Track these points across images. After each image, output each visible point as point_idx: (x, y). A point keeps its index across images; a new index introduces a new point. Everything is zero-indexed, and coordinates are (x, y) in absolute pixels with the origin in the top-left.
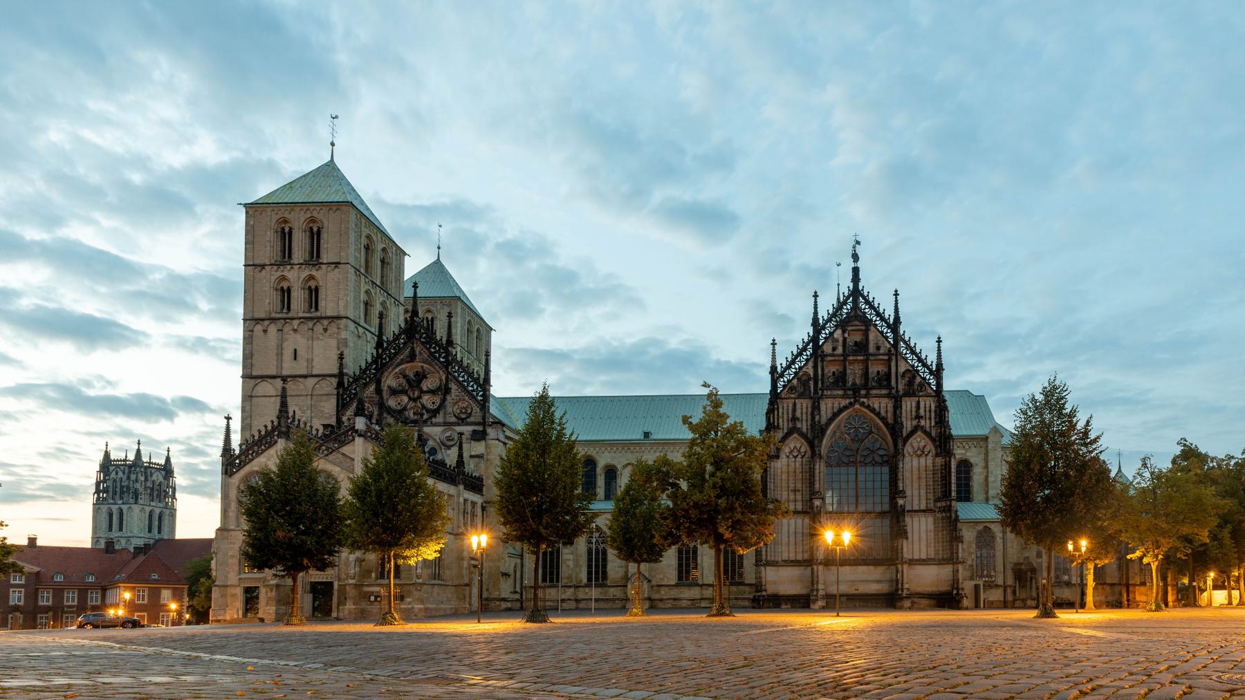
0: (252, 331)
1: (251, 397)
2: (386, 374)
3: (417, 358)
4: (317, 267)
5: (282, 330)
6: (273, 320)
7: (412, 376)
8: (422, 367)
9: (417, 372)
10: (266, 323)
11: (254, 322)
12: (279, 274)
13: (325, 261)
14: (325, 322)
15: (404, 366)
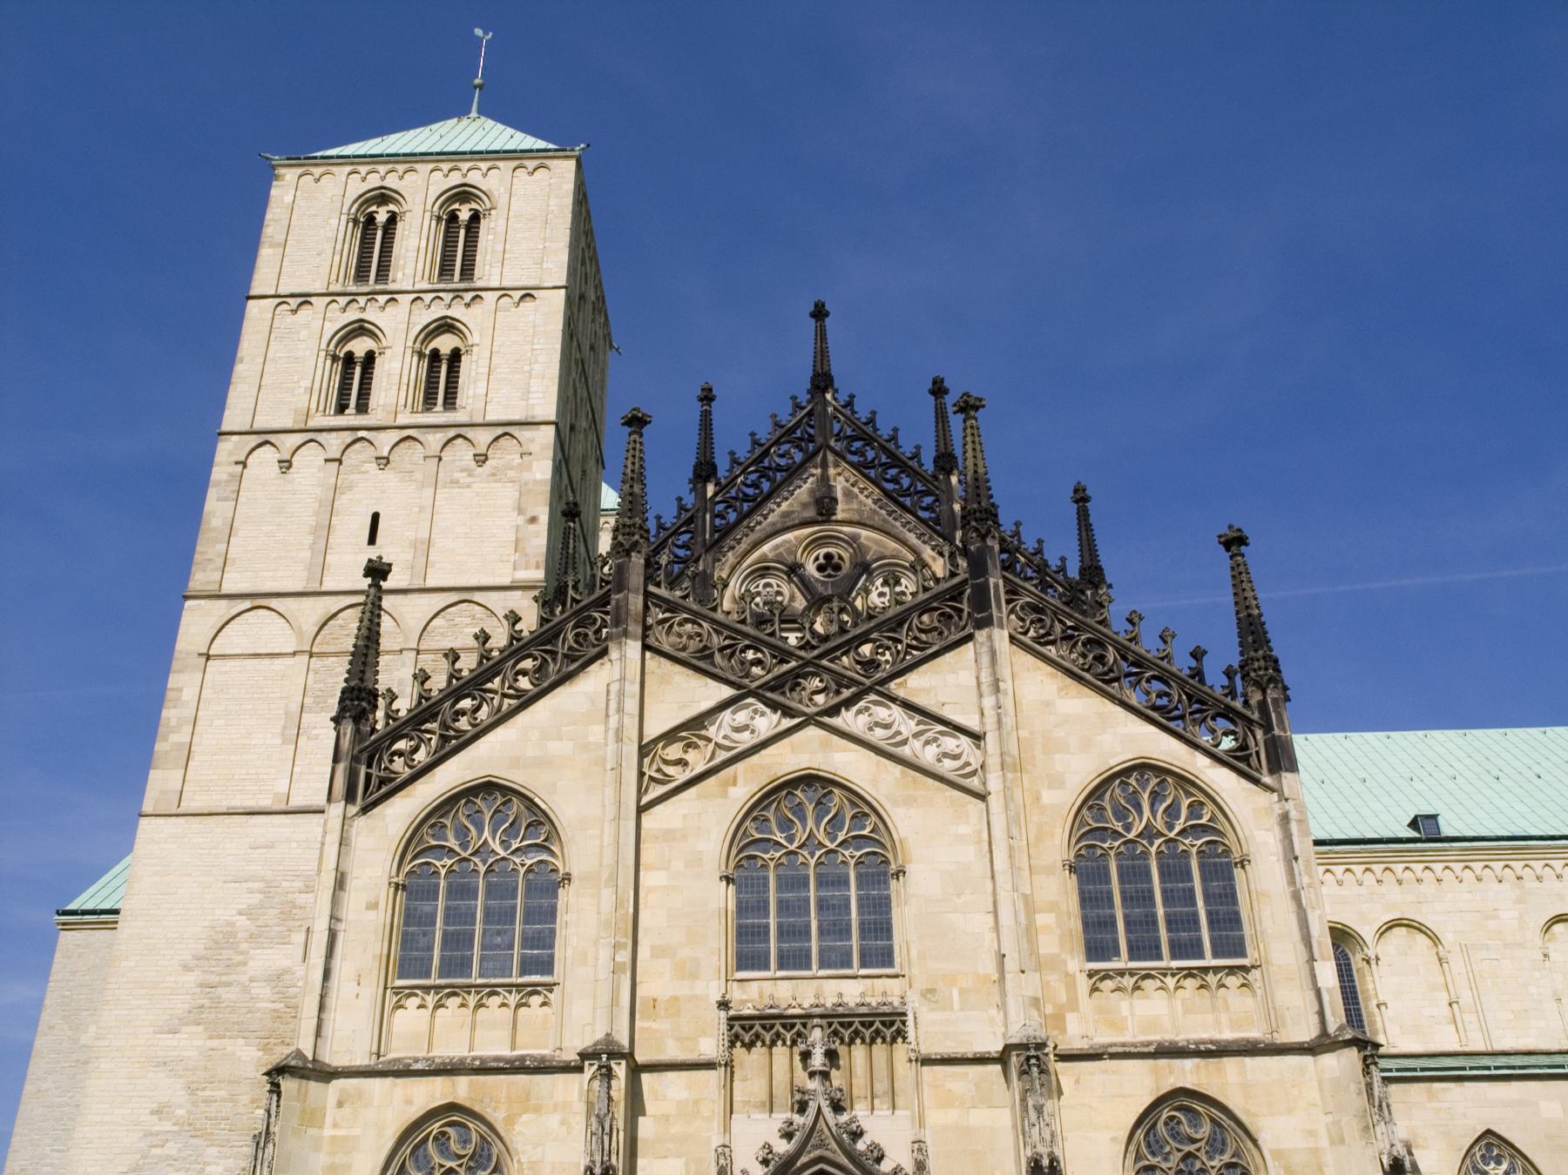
0: (244, 464)
1: (208, 657)
2: (731, 557)
3: (840, 507)
4: (468, 296)
5: (340, 461)
6: (312, 434)
7: (811, 569)
8: (854, 538)
9: (828, 557)
10: (298, 439)
11: (254, 440)
12: (353, 315)
13: (495, 284)
14: (483, 437)
15: (790, 536)
